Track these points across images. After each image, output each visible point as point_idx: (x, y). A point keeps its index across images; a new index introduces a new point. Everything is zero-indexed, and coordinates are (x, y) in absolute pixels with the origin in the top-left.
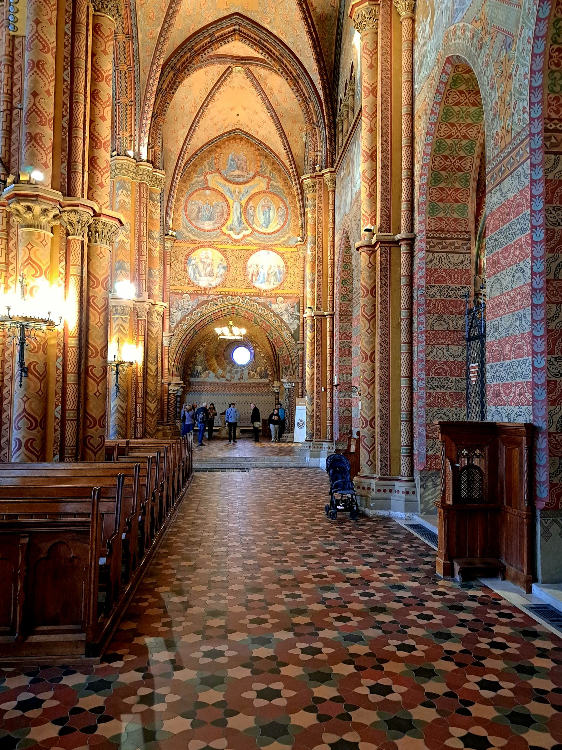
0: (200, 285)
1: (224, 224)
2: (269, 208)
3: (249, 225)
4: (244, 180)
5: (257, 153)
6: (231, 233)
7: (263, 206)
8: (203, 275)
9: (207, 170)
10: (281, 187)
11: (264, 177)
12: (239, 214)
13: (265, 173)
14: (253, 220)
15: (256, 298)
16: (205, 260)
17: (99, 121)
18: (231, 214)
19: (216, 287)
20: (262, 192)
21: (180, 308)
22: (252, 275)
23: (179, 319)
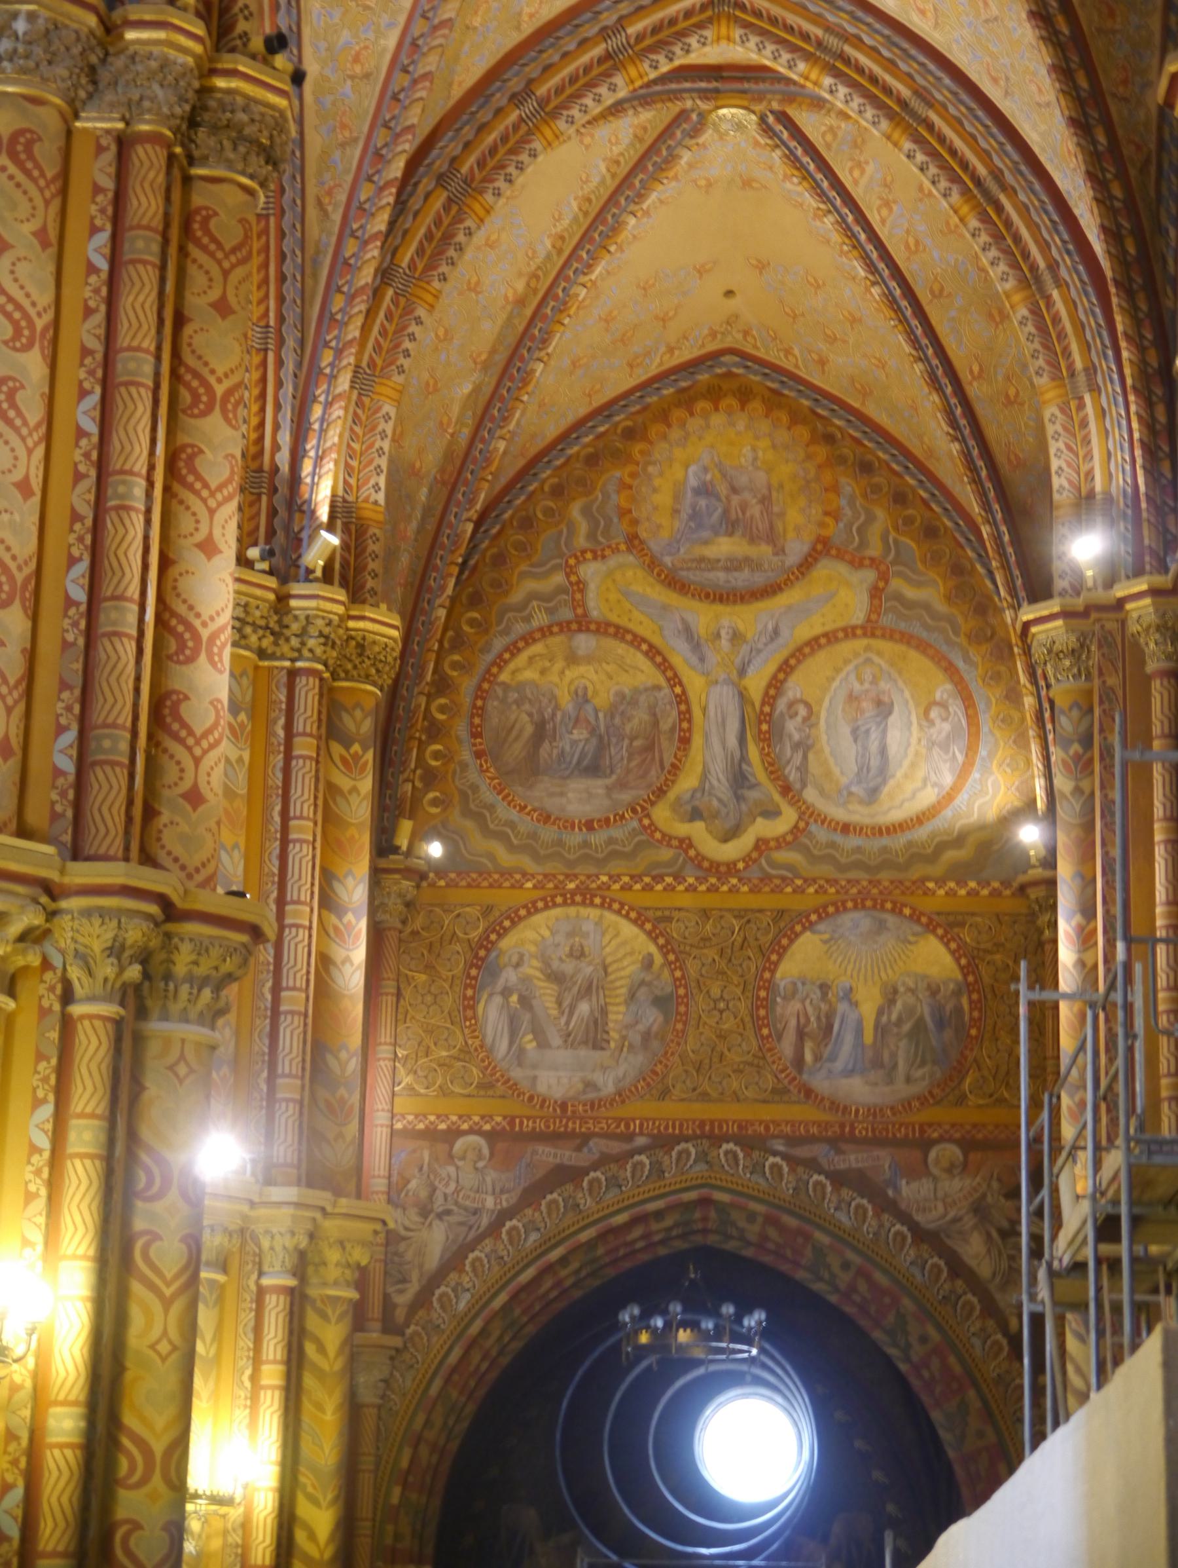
0: (541, 1088)
1: (661, 792)
2: (884, 708)
3: (786, 790)
4: (759, 579)
5: (822, 452)
6: (697, 831)
7: (852, 698)
8: (556, 1041)
9: (581, 541)
10: (941, 607)
11: (857, 563)
12: (732, 741)
13: (863, 544)
14: (803, 769)
15: (819, 1151)
16: (568, 967)
17: (191, 558)
18: (697, 740)
19: (621, 1096)
20: (850, 632)
21: (439, 1204)
22: (801, 1035)
23: (433, 1260)
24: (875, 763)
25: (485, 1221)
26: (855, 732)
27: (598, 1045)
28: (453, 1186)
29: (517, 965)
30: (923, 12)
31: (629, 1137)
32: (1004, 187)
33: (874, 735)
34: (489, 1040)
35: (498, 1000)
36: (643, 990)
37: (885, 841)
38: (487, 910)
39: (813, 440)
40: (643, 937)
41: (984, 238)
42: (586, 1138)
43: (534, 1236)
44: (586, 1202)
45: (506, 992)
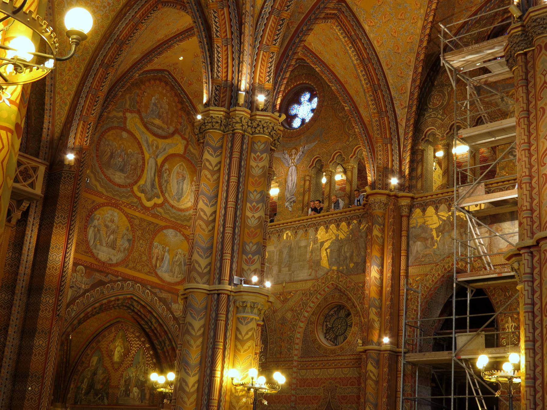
0: (99, 257)
1: (136, 182)
2: (184, 178)
3: (162, 192)
4: (163, 134)
6: (142, 195)
7: (178, 173)
8: (104, 245)
9: (127, 106)
11: (184, 138)
12: (153, 175)
13: (185, 134)
14: (166, 187)
15: (157, 291)
16: (110, 224)
18: (145, 171)
19: (117, 264)
22: (157, 259)
24: (180, 192)
25: (81, 292)
26: (177, 182)
27: (114, 249)
28: (75, 279)
29: (98, 220)
30: (378, 42)
31: (117, 276)
32: (380, 88)
33: (181, 184)
34: (89, 240)
35: (92, 228)
36: (125, 236)
37: (180, 213)
38: (94, 202)
39: (178, 102)
40: (127, 221)
41: (372, 98)
42: (108, 274)
43: (92, 299)
44: (106, 292)
45: (95, 227)
